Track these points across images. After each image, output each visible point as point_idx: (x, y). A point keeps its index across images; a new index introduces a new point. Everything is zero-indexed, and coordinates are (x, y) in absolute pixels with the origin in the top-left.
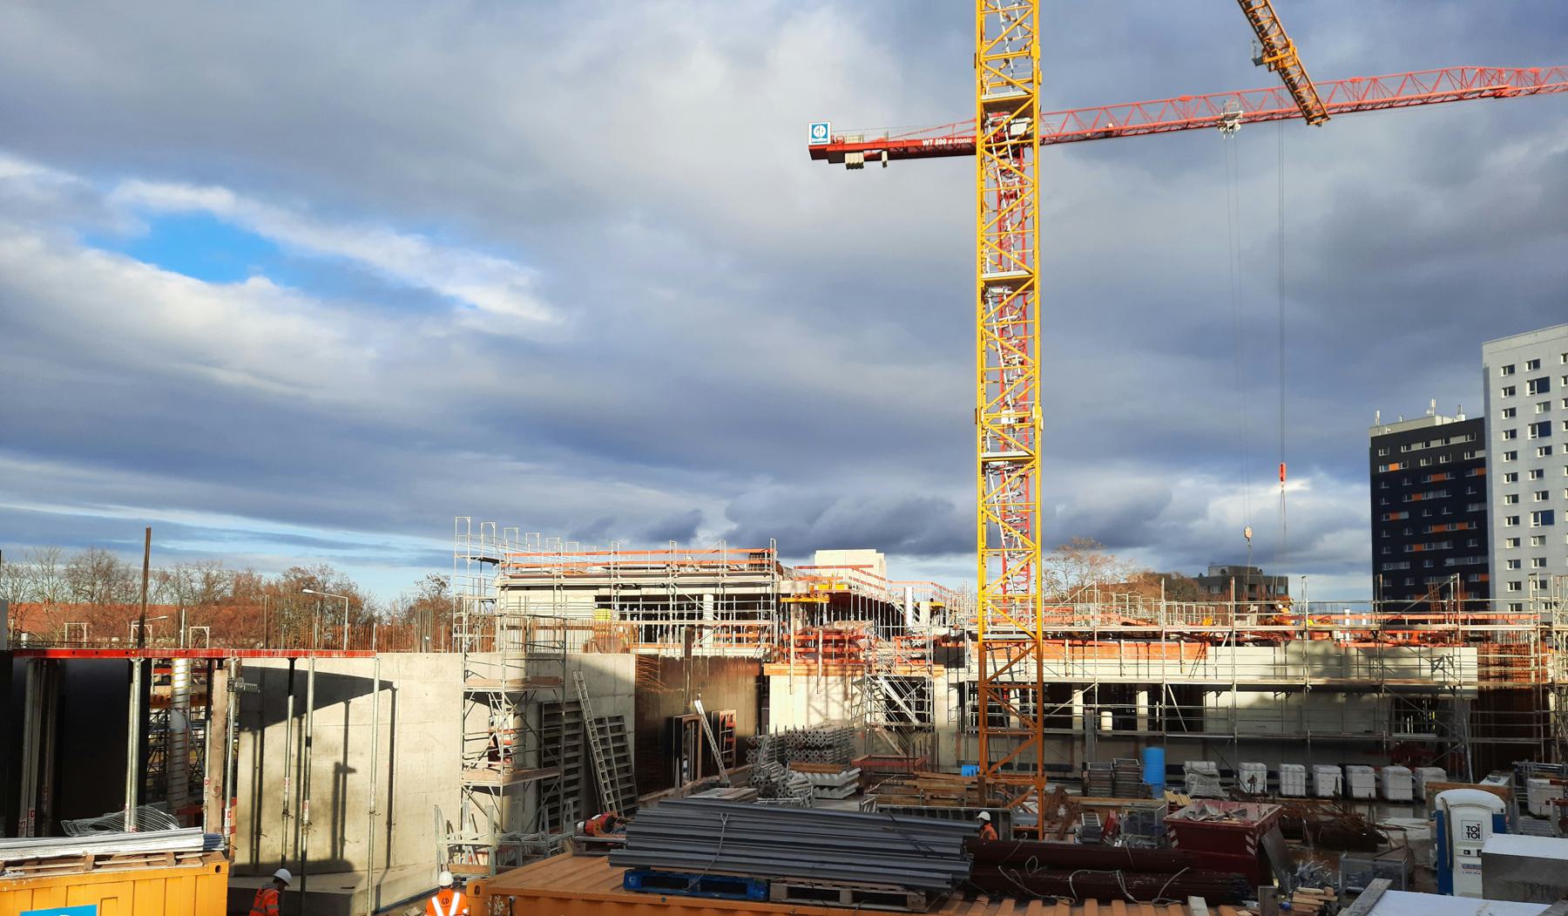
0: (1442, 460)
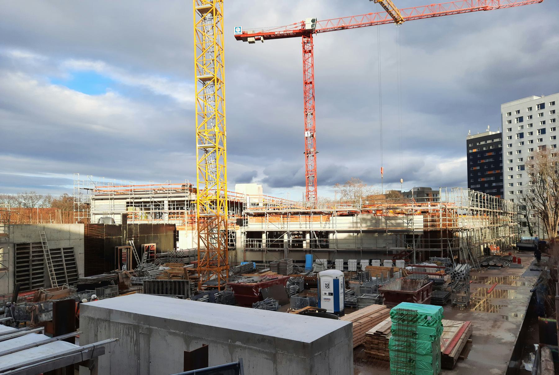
0: (491, 148)
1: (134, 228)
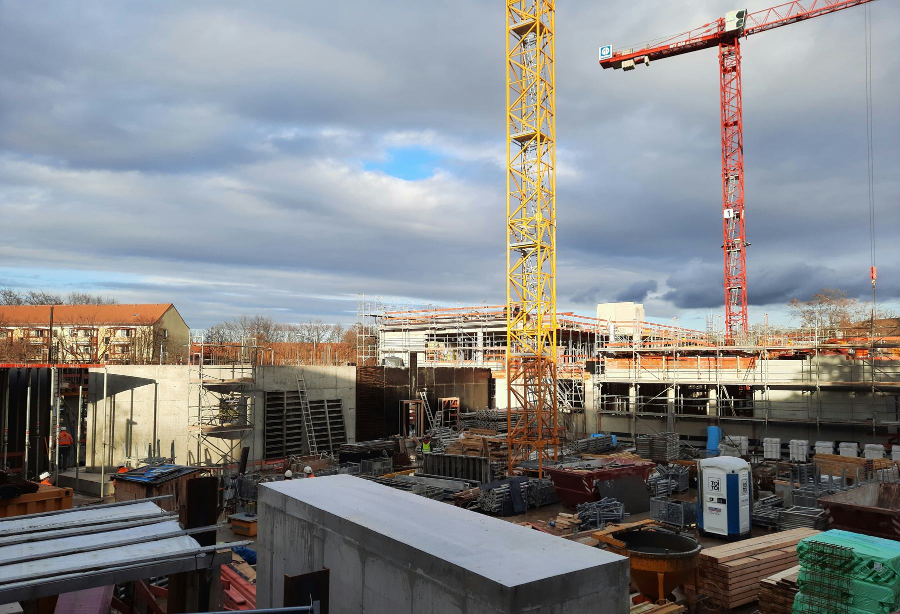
1: (428, 373)
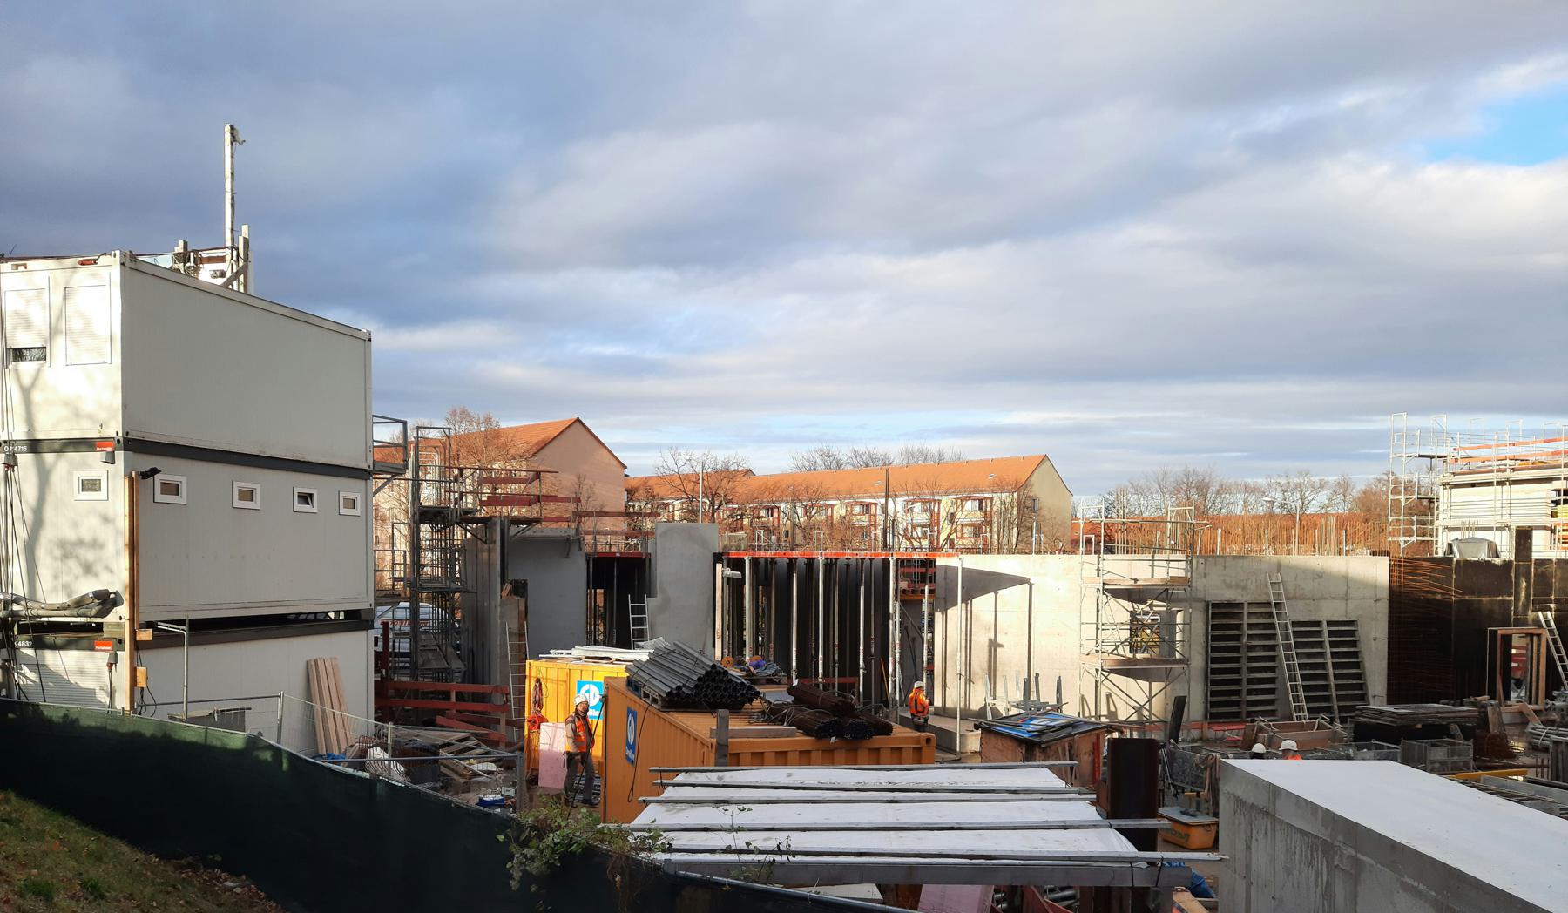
1: (1559, 574)
